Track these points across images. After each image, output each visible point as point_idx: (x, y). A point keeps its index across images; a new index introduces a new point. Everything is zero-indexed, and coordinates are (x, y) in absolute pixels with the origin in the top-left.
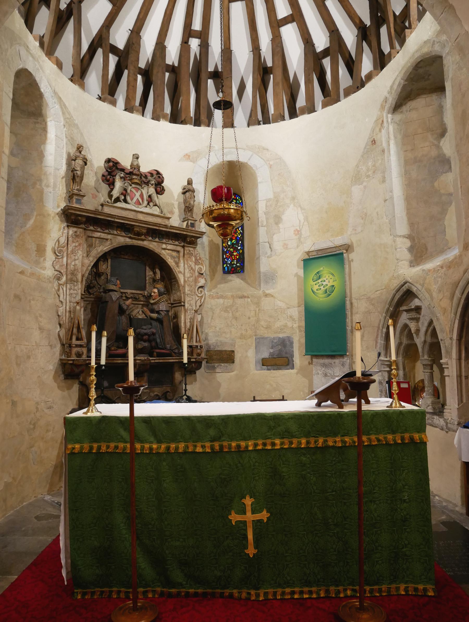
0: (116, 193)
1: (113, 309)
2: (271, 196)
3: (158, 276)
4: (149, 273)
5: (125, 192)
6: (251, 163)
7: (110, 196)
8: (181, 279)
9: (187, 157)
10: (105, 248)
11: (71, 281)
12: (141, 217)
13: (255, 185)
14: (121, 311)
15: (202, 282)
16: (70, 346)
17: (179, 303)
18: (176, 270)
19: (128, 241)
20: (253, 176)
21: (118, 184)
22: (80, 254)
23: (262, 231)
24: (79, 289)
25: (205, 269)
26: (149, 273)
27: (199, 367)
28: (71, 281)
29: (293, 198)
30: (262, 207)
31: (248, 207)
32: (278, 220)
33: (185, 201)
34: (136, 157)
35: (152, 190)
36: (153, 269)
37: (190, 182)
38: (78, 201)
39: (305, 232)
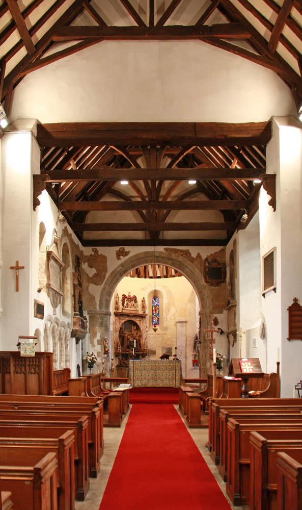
0: (125, 305)
1: (126, 339)
2: (167, 302)
3: (135, 328)
4: (133, 327)
5: (127, 304)
6: (162, 291)
7: (123, 306)
8: (141, 328)
9: (143, 289)
10: (123, 321)
11: (116, 331)
12: (132, 312)
13: (162, 298)
14: (128, 339)
15: (147, 329)
16: (117, 348)
17: (141, 336)
18: (140, 326)
19: (129, 319)
20: (162, 295)
21: (126, 302)
22: (118, 324)
23: (164, 314)
24: (118, 333)
25: (148, 325)
26: (133, 327)
27: (146, 355)
28: (116, 331)
29: (173, 304)
30: (164, 305)
31: (160, 304)
32: (169, 310)
33: (142, 304)
34: (130, 293)
35: (134, 302)
36: (134, 326)
37: (144, 298)
38: (118, 310)
39: (176, 315)
